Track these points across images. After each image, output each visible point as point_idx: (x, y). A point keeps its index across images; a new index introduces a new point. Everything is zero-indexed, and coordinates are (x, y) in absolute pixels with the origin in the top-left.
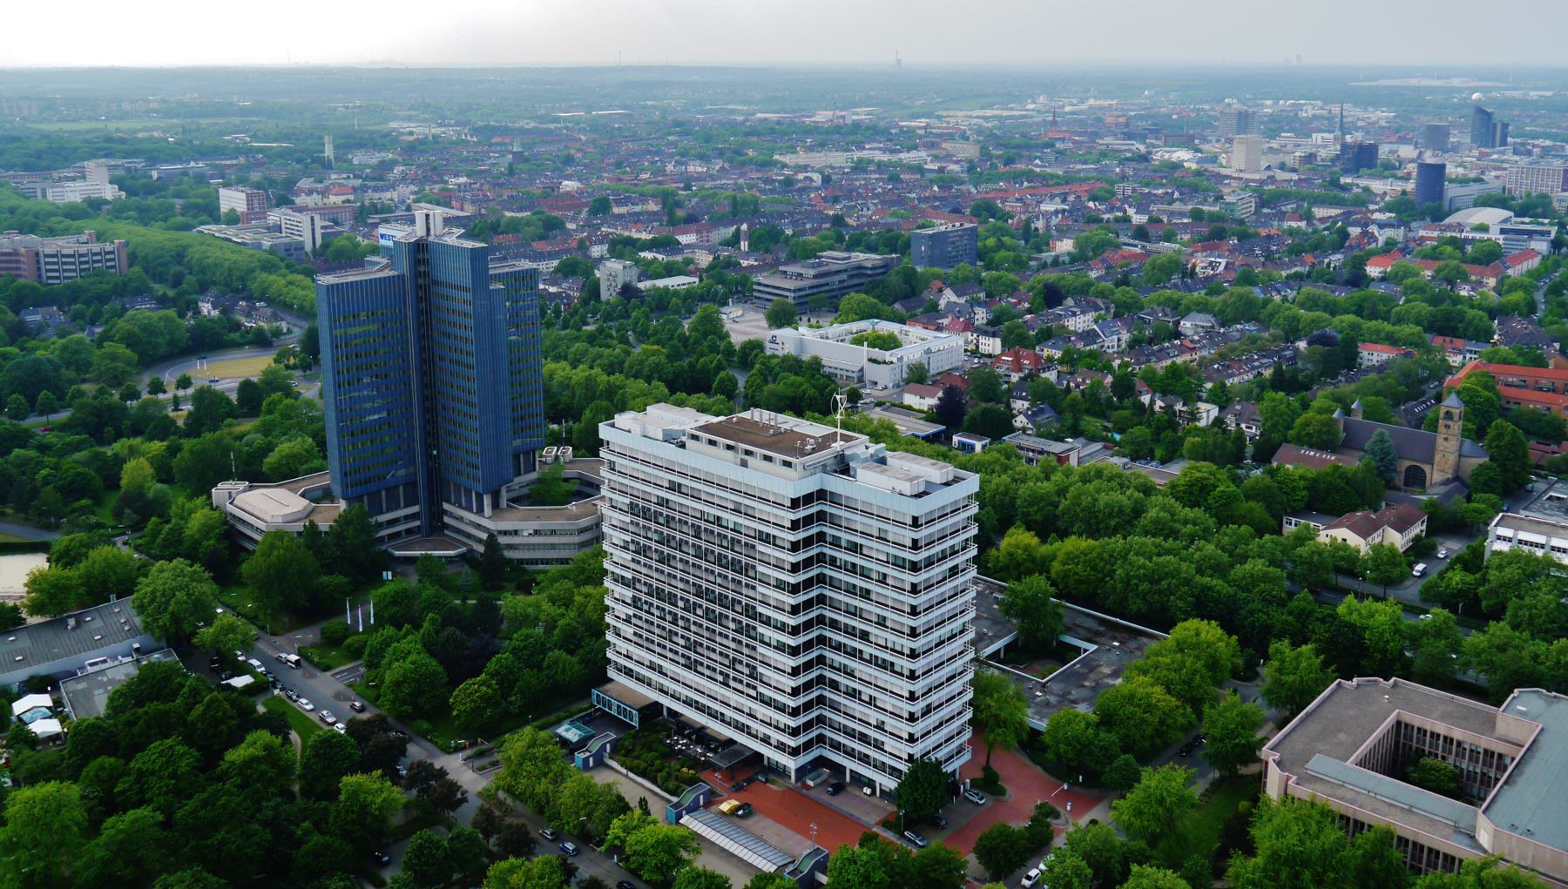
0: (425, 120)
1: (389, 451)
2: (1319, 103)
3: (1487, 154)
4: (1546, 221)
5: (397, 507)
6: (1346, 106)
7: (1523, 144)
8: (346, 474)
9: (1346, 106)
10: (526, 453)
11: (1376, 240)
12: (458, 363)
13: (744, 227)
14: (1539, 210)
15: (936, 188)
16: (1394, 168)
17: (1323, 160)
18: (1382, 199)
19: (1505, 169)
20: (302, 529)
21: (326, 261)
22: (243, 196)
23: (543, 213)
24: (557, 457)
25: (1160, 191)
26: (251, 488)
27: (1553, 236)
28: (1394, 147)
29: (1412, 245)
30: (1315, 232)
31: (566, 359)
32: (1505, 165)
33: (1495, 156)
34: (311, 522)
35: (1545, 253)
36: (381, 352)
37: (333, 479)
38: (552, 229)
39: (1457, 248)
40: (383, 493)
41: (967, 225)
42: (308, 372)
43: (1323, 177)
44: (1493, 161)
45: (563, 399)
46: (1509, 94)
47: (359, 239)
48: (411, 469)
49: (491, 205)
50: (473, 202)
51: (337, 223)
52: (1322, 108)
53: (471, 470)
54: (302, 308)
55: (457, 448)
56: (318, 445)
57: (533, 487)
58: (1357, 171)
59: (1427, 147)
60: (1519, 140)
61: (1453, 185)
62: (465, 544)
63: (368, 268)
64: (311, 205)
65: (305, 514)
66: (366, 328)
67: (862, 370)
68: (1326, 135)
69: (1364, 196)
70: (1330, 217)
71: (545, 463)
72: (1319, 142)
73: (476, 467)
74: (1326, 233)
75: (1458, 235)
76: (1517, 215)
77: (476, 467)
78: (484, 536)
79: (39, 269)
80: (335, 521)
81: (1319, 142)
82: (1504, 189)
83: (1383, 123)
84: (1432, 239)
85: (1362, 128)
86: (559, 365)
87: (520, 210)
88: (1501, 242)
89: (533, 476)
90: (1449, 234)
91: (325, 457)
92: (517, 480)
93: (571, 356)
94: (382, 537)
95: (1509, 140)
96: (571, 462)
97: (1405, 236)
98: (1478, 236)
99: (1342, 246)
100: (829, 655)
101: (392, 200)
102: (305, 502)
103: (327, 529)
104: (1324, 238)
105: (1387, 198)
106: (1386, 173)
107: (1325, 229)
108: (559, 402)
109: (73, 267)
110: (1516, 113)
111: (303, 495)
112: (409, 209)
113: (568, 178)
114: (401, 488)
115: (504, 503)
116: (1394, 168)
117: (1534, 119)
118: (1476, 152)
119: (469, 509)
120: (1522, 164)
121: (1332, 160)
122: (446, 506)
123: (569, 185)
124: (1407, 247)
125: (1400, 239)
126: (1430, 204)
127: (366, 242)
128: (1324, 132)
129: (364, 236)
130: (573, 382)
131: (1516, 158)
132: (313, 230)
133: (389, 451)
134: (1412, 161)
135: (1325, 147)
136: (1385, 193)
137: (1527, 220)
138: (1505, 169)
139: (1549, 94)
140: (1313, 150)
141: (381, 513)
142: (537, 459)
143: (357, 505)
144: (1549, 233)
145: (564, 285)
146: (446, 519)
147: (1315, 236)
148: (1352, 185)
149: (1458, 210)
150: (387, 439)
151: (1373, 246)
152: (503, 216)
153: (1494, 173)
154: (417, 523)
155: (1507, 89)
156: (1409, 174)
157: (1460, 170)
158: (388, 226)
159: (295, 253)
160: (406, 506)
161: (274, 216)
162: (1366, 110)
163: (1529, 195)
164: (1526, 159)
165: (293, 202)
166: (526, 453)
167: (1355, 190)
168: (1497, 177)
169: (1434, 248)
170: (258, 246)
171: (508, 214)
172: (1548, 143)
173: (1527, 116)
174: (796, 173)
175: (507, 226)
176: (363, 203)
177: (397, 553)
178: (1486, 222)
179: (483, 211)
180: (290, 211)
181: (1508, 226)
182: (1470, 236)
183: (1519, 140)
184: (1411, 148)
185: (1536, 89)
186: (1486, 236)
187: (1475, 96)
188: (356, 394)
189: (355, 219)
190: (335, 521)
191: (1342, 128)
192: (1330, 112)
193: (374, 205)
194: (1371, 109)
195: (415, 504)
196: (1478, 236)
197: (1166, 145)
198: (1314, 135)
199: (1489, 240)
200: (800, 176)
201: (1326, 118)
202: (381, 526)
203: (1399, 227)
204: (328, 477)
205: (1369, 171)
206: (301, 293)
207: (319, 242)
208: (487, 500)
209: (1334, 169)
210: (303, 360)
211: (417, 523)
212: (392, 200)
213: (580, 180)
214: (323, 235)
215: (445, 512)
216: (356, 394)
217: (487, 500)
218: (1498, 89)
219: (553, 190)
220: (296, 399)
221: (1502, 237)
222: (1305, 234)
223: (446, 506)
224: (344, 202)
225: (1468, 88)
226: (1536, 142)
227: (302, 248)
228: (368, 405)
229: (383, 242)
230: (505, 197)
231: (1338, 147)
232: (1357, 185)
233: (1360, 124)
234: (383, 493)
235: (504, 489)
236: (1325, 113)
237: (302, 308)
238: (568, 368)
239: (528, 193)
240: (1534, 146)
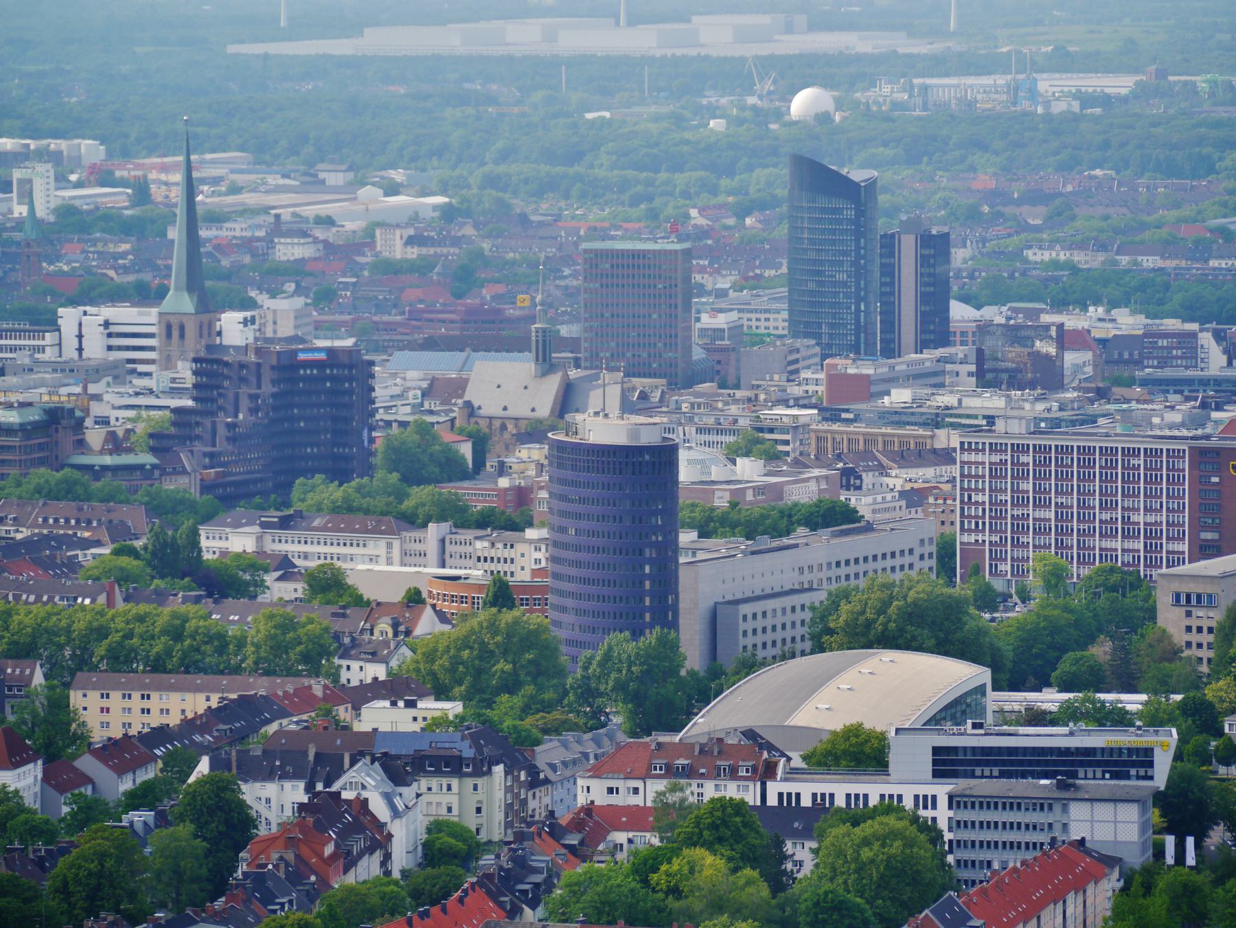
2: (90, 149)
3: (865, 389)
4: (1133, 702)
6: (211, 164)
7: (1015, 334)
9: (211, 164)
11: (380, 841)
14: (1101, 651)
16: (452, 469)
17: (115, 444)
18: (403, 630)
19: (946, 456)
27: (1160, 779)
28: (445, 364)
29: (542, 856)
30: (90, 812)
32: (947, 438)
33: (900, 396)
35: (1136, 859)
39: (749, 858)
43: (119, 532)
44: (897, 417)
46: (946, 87)
52: (102, 177)
58: (285, 487)
59: (594, 362)
60: (995, 314)
61: (719, 546)
68: (125, 314)
69: (318, 618)
70: (160, 735)
72: (95, 348)
74: (139, 818)
75: (751, 796)
76: (1009, 680)
81: (95, 348)
82: (945, 554)
83: (395, 247)
84: (635, 818)
85: (297, 270)
88: (942, 815)
90: (710, 791)
95: (959, 312)
97: (516, 809)
98: (840, 789)
99: (219, 884)
104: (130, 841)
105: (426, 624)
106: (419, 495)
107: (136, 799)
110: (985, 180)
116: (452, 469)
117: (1061, 214)
118: (814, 381)
120: (1013, 429)
121: (160, 442)
124: (522, 865)
125: (494, 827)
126: (622, 644)
128: (116, 296)
131: (992, 401)
134: (532, 433)
135: (121, 372)
136: (414, 599)
137: (1050, 699)
138: (946, 456)
139: (1120, 84)
140: (68, 393)
144: (1143, 759)
147: (87, 842)
148: (256, 564)
149: (749, 666)
151: (368, 868)
153: (898, 479)
155: (939, 65)
156: (522, 496)
157: (749, 469)
162: (313, 183)
163: (1055, 579)
164: (1033, 406)
167: (280, 591)
168: (913, 497)
169: (646, 866)
172: (1128, 322)
173: (1035, 198)
178: (874, 722)
181: (967, 738)
182: (806, 791)
183: (995, 314)
184: (520, 367)
185: (1063, 62)
186: (873, 790)
187: (803, 102)
191: (194, 282)
192: (141, 192)
194: (335, 178)
196: (840, 789)
198: (68, 317)
199: (890, 806)
201: (127, 228)
203: (481, 768)
205: (335, 492)
209: (171, 485)
218: (904, 66)
221: (942, 790)
222: (38, 830)
225: (768, 64)
226: (1073, 321)
231: (185, 372)
232: (286, 568)
233: (289, 251)
236: (115, 198)
240: (1065, 339)
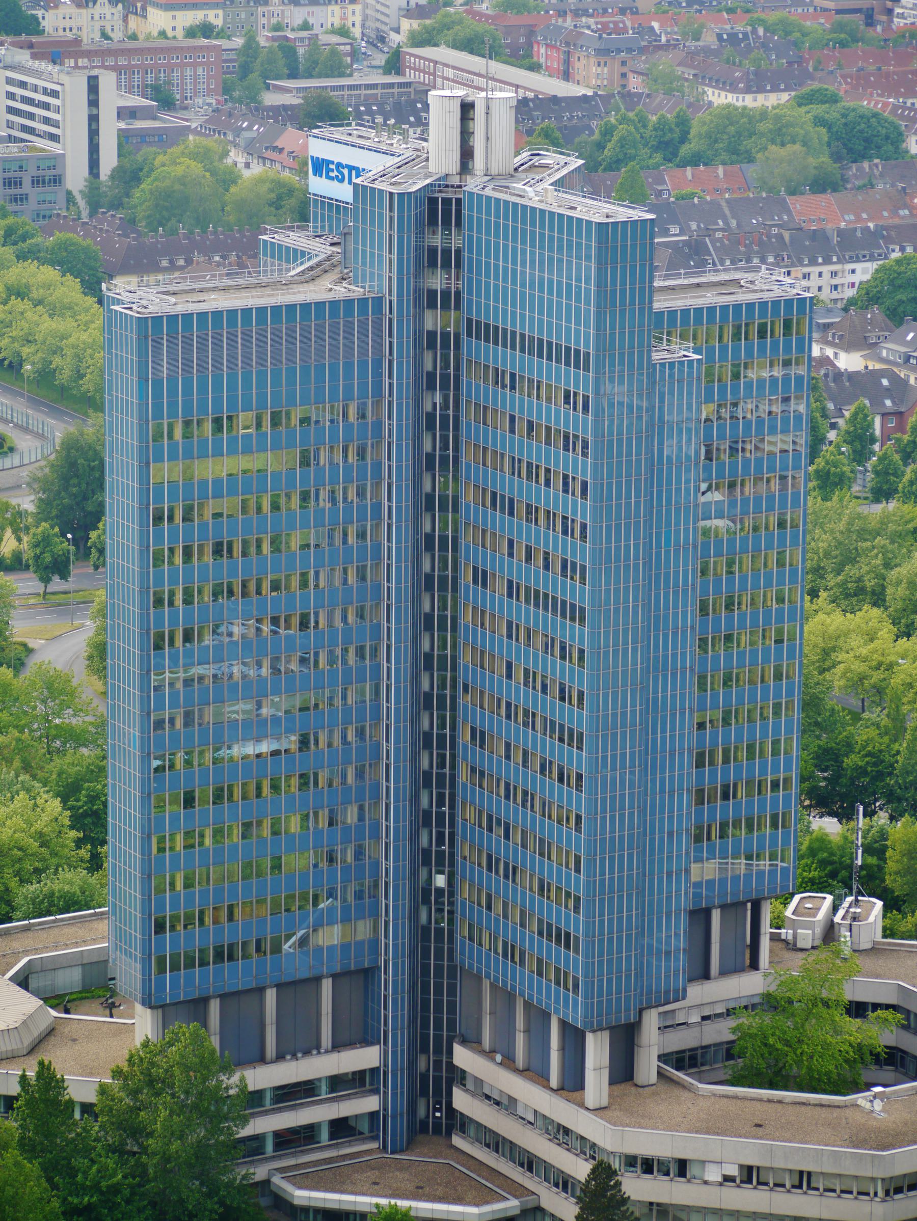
1: (296, 862)
5: (311, 1047)
8: (160, 927)
10: (731, 908)
12: (537, 598)
20: (14, 1089)
21: (130, 223)
23: (834, 100)
31: (878, 599)
34: (45, 1070)
36: (295, 542)
37: (119, 936)
38: (858, 157)
40: (271, 996)
42: (57, 584)
45: (863, 734)
47: (236, 157)
48: (363, 930)
49: (665, 62)
50: (603, 52)
51: (167, 103)
53: (554, 953)
54: (46, 375)
55: (511, 872)
56: (77, 822)
57: (745, 1020)
62: (517, 1190)
63: (270, 269)
64: (90, 36)
65: (27, 1041)
66: (252, 463)
71: (792, 946)
73: (566, 940)
77: (566, 940)
78: (580, 1169)
80: (117, 1073)
86: (856, 620)
87: (756, 85)
91: (95, 864)
92: (697, 993)
93: (896, 594)
94: (258, 1139)
96: (875, 950)
101: (343, 32)
102: (29, 1003)
103: (90, 1096)
108: (849, 746)
111: (23, 981)
112: (395, 64)
127: (257, 169)
129: (250, 149)
130: (897, 680)
132: (93, 119)
133: (296, 862)
141: (262, 1059)
142: (766, 929)
143: (186, 1029)
145: (891, 349)
146: (461, 1101)
150: (294, 825)
152: (697, 105)
154: (371, 1104)
158: (339, 133)
159: (34, 194)
160: (338, 1046)
165: (33, 27)
166: (731, 908)
171: (719, 98)
175: (712, 138)
176: (251, 41)
177: (302, 1196)
179: (635, 83)
180: (23, 57)
188: (208, 670)
189: (227, 89)
190: (117, 1073)
193: (288, 50)
195: (366, 1041)
202: (254, 1100)
204: (103, 927)
206: (48, 325)
207: (109, 160)
210: (44, 542)
211: (371, 1104)
212: (343, 32)
214: (124, 137)
215: (458, 1076)
216: (208, 670)
219: (870, 21)
220: (18, 665)
223: (463, 1057)
224: (191, 33)
227: (57, 180)
228: (238, 710)
229: (318, 185)
230: (709, 39)
234: (271, 996)
235: (651, 1020)
237: (46, 375)
238: (886, 631)
239: (786, 28)
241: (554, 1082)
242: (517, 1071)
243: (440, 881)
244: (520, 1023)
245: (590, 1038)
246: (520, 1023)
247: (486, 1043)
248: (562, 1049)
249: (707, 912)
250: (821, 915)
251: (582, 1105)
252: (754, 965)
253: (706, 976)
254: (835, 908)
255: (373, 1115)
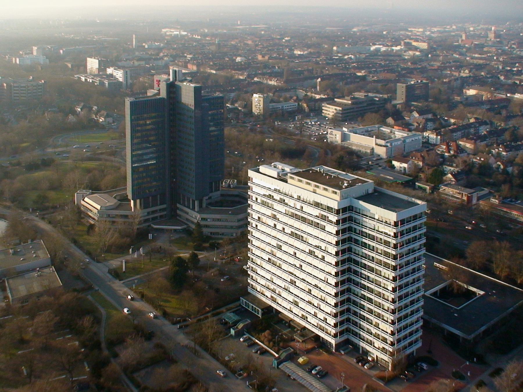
0: (178, 29)
5: (157, 205)
13: (319, 80)
15: (409, 64)
22: (97, 61)
24: (229, 185)
25: (515, 69)
26: (92, 193)
40: (150, 198)
41: (424, 81)
62: (186, 224)
67: (373, 149)
79: (11, 93)
89: (219, 193)
100: (353, 287)
102: (116, 201)
109: (25, 92)
111: (115, 198)
113: (240, 56)
114: (159, 196)
115: (204, 205)
119: (189, 207)
122: (178, 205)
123: (239, 59)
142: (221, 185)
154: (165, 213)
160: (161, 204)
161: (110, 71)
170: (102, 84)
174: (344, 55)
197: (517, 48)
200: (346, 57)
208: (196, 203)
211: (165, 213)
213: (245, 57)
215: (178, 208)
217: (196, 203)
223: (178, 205)
234: (150, 198)
241: (191, 207)
242: (186, 207)
243: (174, 180)
244: (186, 200)
245: (196, 201)
246: (186, 200)
247: (181, 203)
248: (192, 204)
249: (212, 183)
250: (228, 183)
251: (195, 211)
252: (219, 190)
253: (212, 192)
254: (230, 181)
255: (166, 214)
